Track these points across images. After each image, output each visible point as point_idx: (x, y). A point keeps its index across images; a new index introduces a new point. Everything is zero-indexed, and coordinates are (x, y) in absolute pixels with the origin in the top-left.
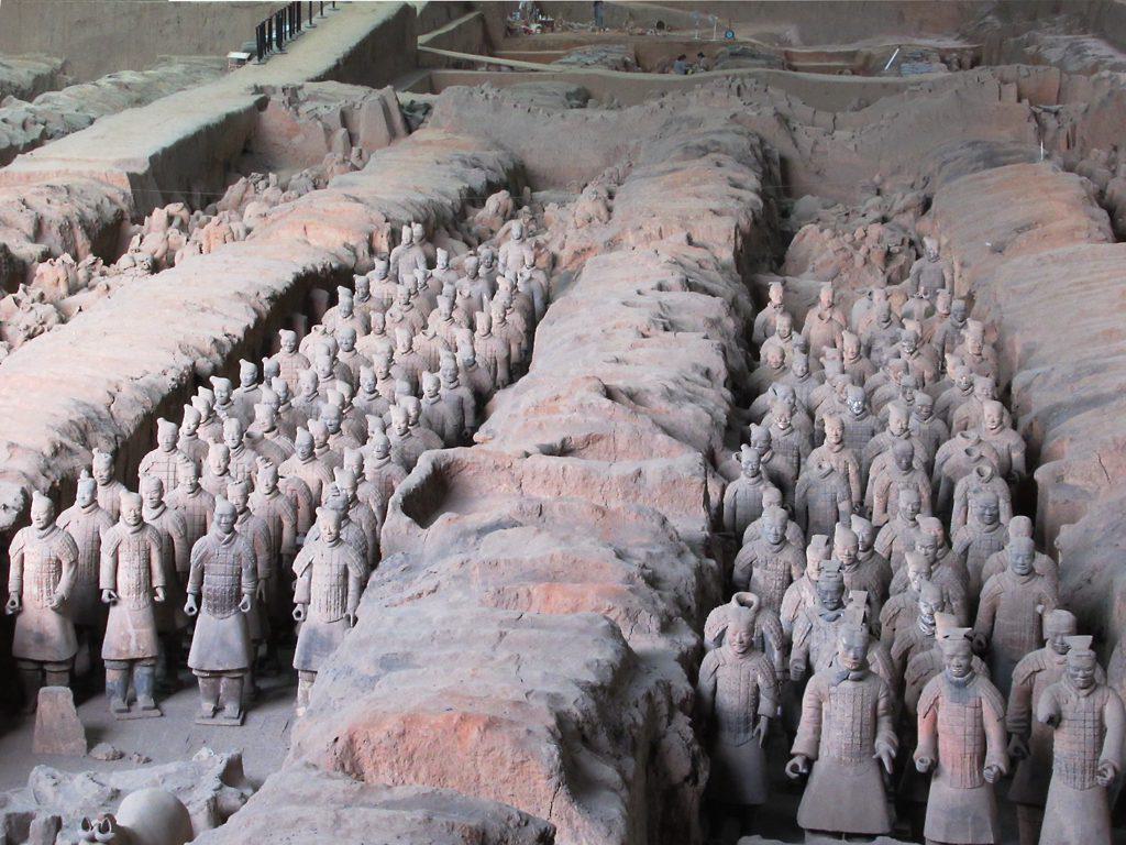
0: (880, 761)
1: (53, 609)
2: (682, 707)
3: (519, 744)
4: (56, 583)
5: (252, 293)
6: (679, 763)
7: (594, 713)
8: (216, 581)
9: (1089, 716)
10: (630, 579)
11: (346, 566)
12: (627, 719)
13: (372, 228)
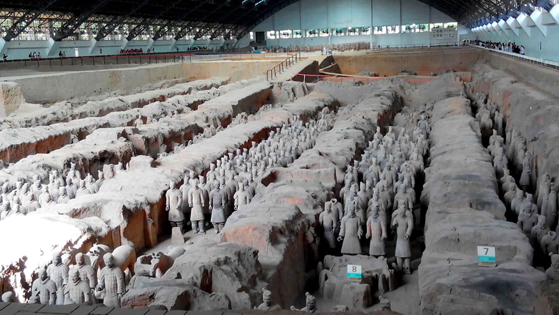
0: (358, 236)
1: (177, 209)
2: (313, 225)
3: (260, 233)
4: (177, 203)
5: (249, 133)
6: (310, 238)
7: (285, 227)
8: (216, 201)
9: (404, 224)
10: (308, 196)
11: (246, 197)
12: (295, 228)
13: (289, 117)
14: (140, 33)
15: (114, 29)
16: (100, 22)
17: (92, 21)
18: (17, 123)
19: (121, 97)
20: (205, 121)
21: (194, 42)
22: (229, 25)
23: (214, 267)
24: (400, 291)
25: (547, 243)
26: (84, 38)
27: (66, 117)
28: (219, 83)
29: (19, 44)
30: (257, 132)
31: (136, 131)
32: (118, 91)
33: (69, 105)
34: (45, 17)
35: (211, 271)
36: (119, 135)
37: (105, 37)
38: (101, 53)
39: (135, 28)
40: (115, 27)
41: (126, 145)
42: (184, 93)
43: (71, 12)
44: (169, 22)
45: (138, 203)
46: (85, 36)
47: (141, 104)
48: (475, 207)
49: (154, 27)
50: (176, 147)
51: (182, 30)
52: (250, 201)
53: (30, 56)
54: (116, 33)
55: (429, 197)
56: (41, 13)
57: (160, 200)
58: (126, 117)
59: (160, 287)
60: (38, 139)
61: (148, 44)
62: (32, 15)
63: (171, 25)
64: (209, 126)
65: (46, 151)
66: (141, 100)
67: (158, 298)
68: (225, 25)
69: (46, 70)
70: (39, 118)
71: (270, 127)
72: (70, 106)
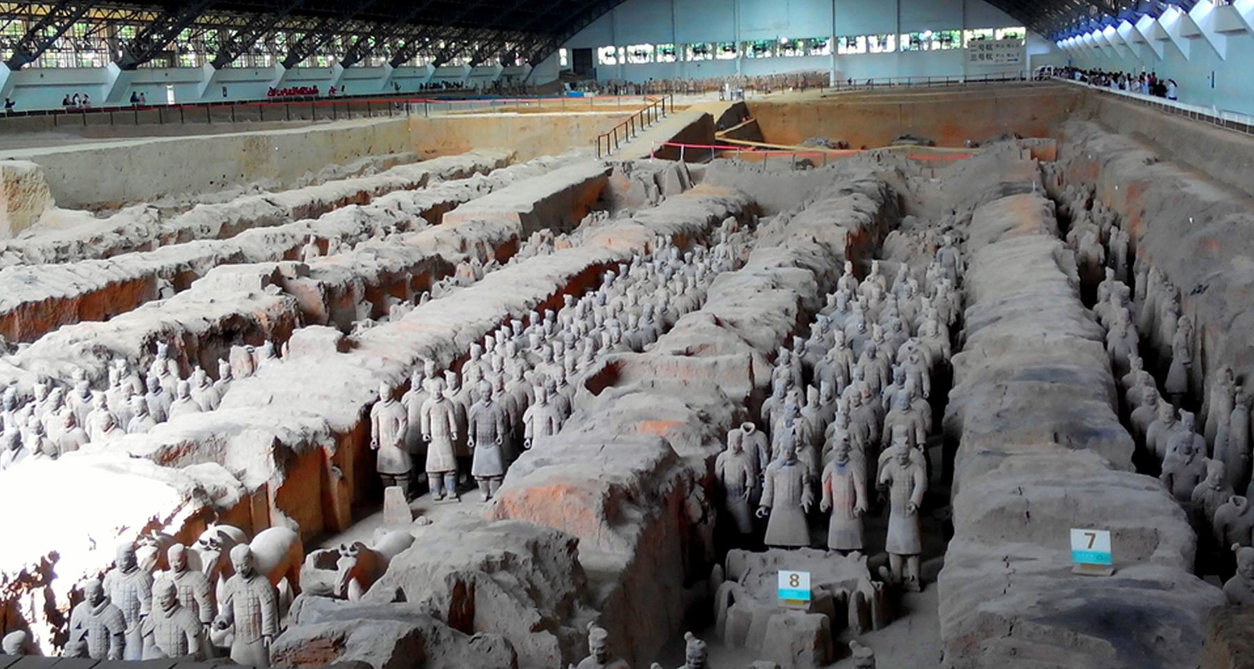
14: (312, 51)
15: (254, 43)
16: (222, 28)
17: (204, 26)
18: (36, 253)
19: (270, 196)
20: (459, 247)
21: (435, 72)
22: (512, 33)
23: (480, 575)
24: (897, 630)
25: (1227, 521)
26: (187, 63)
27: (147, 240)
28: (491, 164)
29: (42, 76)
30: (575, 273)
31: (303, 271)
32: (263, 182)
33: (154, 212)
34: (99, 15)
35: (473, 585)
36: (266, 281)
37: (234, 59)
38: (225, 96)
39: (300, 41)
40: (257, 37)
41: (281, 303)
42: (411, 187)
43: (159, 5)
44: (378, 27)
45: (308, 431)
46: (190, 59)
47: (314, 210)
48: (1065, 440)
49: (345, 38)
50: (394, 307)
51: (407, 44)
52: (560, 428)
53: (65, 103)
54: (259, 52)
55: (963, 419)
56: (91, 6)
57: (359, 425)
58: (282, 239)
59: (358, 620)
60: (84, 290)
61: (330, 76)
62: (70, 10)
63: (383, 34)
64: (467, 260)
65: (103, 316)
66: (316, 202)
67: (352, 646)
68: (504, 33)
69: (102, 135)
70: (86, 241)
71: (604, 262)
72: (156, 216)
